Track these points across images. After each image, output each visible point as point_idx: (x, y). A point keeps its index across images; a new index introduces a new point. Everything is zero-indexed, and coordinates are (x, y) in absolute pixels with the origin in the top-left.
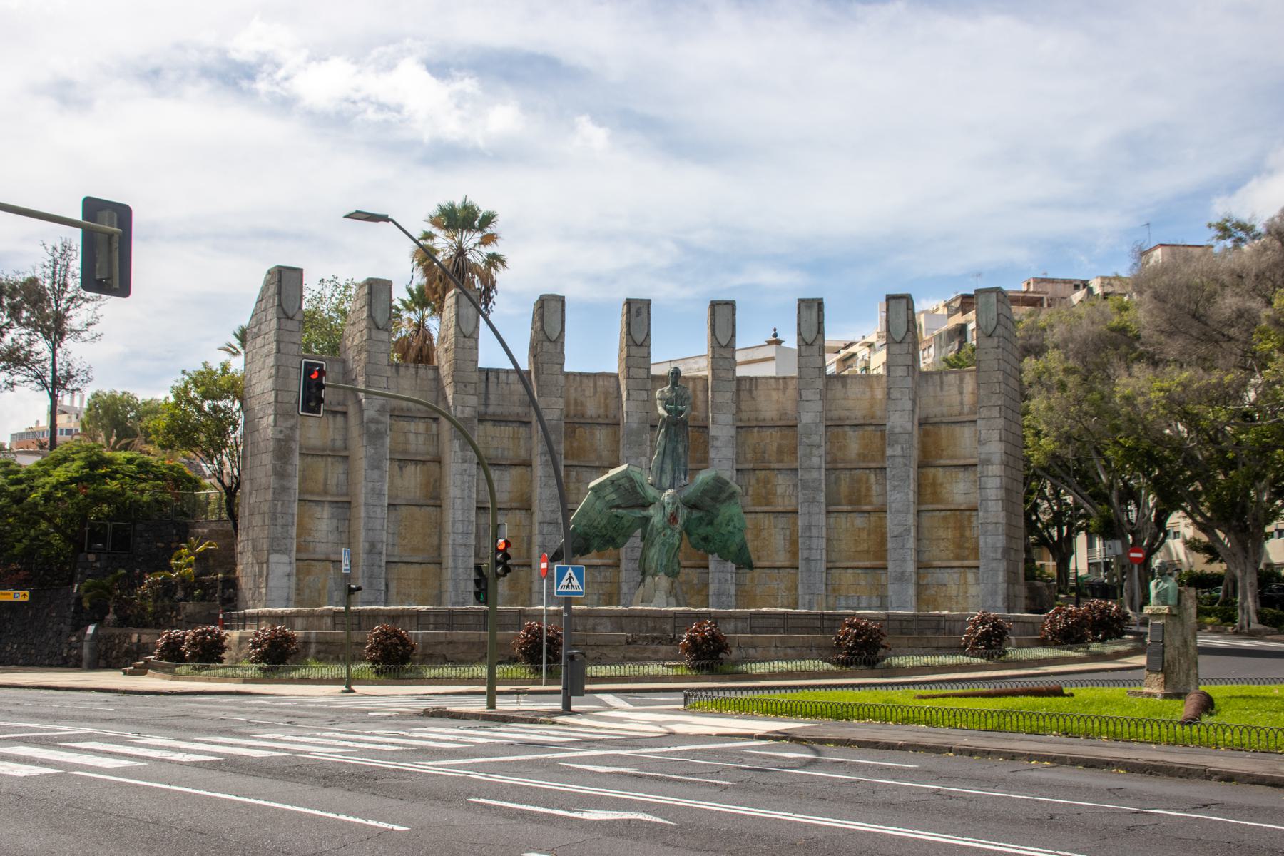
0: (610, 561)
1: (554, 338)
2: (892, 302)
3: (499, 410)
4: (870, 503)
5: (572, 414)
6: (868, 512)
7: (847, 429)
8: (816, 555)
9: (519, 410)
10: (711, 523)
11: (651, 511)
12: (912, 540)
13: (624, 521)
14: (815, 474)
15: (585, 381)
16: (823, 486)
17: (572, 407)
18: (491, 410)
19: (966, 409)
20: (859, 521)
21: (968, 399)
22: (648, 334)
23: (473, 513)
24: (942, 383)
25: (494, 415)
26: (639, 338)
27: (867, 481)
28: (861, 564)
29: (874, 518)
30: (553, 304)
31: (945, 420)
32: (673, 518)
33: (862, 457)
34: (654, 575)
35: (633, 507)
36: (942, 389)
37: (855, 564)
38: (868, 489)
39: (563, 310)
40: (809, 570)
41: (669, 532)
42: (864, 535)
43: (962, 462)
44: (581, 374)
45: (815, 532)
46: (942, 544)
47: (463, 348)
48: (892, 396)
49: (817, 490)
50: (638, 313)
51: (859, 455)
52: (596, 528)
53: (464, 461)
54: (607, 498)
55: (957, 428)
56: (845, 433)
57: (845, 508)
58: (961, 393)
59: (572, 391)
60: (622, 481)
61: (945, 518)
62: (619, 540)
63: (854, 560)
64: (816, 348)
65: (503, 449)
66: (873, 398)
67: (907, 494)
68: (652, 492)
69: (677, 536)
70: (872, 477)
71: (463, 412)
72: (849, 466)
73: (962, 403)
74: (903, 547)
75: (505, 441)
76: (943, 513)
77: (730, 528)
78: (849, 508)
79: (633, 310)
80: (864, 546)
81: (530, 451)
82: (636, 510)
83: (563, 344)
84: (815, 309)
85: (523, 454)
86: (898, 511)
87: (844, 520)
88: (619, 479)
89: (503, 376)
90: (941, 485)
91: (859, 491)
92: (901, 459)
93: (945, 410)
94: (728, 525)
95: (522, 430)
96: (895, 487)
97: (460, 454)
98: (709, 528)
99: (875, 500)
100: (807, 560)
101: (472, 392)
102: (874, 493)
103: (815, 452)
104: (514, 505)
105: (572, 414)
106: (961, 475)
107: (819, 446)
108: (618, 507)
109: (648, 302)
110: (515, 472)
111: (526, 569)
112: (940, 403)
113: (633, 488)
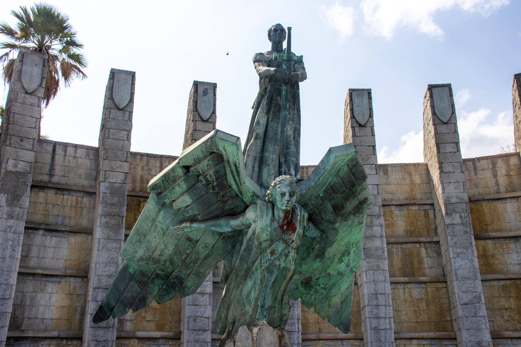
0: (171, 334)
1: (122, 106)
2: (434, 90)
3: (64, 181)
4: (424, 275)
5: (138, 189)
6: (425, 283)
7: (393, 208)
8: (384, 324)
9: (86, 183)
10: (321, 255)
11: (250, 214)
12: (484, 307)
13: (200, 247)
14: (377, 243)
15: (152, 161)
16: (386, 254)
17: (138, 184)
18: (55, 179)
19: (502, 189)
20: (417, 292)
21: (502, 180)
22: (214, 112)
23: (15, 276)
24: (475, 168)
25: (58, 184)
26: (206, 115)
27: (419, 254)
28: (425, 335)
29: (430, 288)
30: (124, 76)
31: (486, 197)
32: (288, 223)
33: (410, 233)
34: (250, 325)
35: (217, 217)
36: (476, 174)
37: (417, 335)
38: (420, 262)
39: (133, 84)
40: (379, 340)
41: (280, 247)
42: (423, 305)
43: (512, 234)
44: (148, 155)
45: (381, 300)
46: (506, 315)
47: (24, 103)
48: (446, 170)
49: (380, 258)
50: (205, 93)
51: (406, 231)
52: (156, 261)
53: (10, 217)
54: (178, 204)
55: (499, 205)
56: (391, 212)
57: (402, 279)
58: (495, 176)
59: (139, 169)
60: (204, 166)
61: (505, 286)
62: (189, 283)
63: (415, 331)
64: (369, 129)
65: (64, 217)
66: (412, 183)
67: (472, 261)
68: (249, 185)
69: (293, 253)
70: (423, 250)
71: (15, 166)
72: (400, 240)
73: (497, 184)
74: (475, 315)
75: (67, 209)
76: (502, 283)
77: (342, 267)
78: (406, 279)
79: (200, 90)
80: (424, 317)
81: (92, 221)
82: (222, 222)
83: (131, 113)
84: (367, 96)
85: (84, 222)
86: (464, 278)
87: (401, 291)
88: (198, 161)
89: (70, 150)
90: (493, 256)
91: (412, 264)
92: (461, 228)
93: (481, 190)
94: (341, 261)
95: (86, 200)
96: (458, 254)
97: (6, 209)
98: (317, 264)
99: (427, 271)
100: (376, 329)
101: (29, 147)
102: (426, 265)
103: (376, 222)
104: (69, 272)
105: (138, 189)
106: (512, 246)
107: (379, 216)
108: (193, 220)
109: (215, 86)
110: (75, 240)
111: (75, 342)
112: (476, 186)
113: (221, 177)
